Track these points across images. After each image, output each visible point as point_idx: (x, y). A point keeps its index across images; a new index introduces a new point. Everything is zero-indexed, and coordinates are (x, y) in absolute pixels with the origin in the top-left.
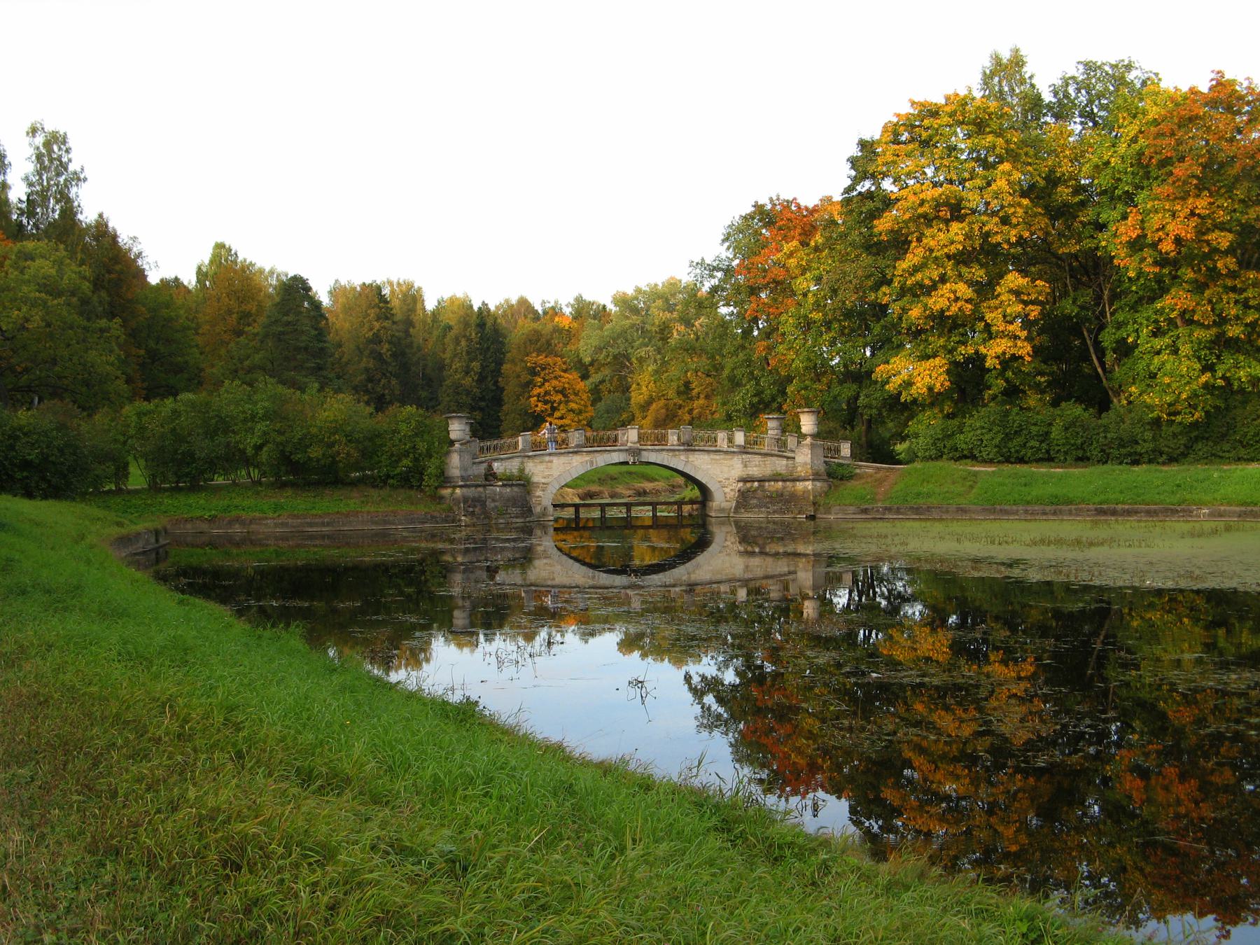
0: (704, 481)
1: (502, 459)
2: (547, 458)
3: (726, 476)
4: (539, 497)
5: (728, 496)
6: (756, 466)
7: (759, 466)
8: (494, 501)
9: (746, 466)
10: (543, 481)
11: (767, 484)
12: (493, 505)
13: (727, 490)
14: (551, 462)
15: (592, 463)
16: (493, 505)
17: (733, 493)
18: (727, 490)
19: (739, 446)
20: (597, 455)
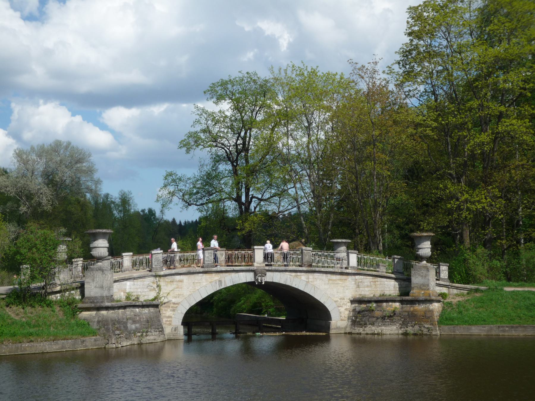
0: (322, 301)
1: (135, 278)
2: (178, 278)
3: (341, 296)
4: (169, 317)
5: (343, 315)
6: (368, 286)
7: (371, 286)
8: (134, 322)
9: (358, 286)
10: (174, 300)
11: (385, 304)
12: (133, 327)
13: (342, 309)
14: (181, 281)
15: (220, 281)
16: (133, 327)
17: (347, 312)
18: (342, 309)
19: (353, 268)
20: (224, 274)
